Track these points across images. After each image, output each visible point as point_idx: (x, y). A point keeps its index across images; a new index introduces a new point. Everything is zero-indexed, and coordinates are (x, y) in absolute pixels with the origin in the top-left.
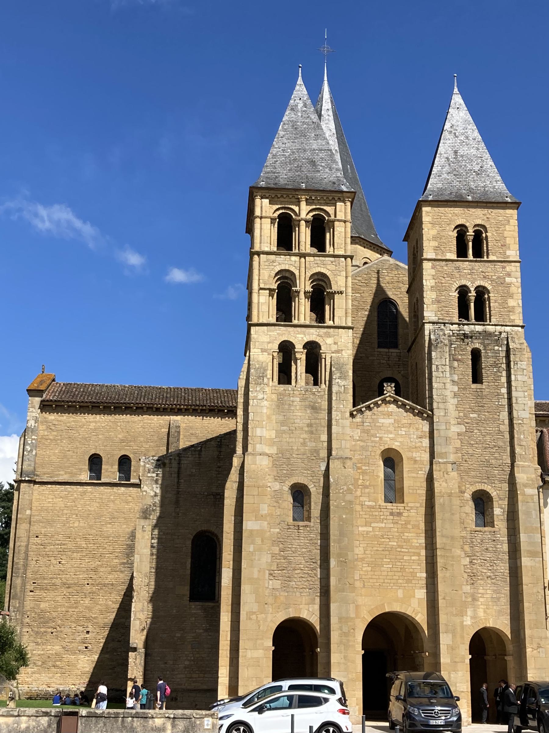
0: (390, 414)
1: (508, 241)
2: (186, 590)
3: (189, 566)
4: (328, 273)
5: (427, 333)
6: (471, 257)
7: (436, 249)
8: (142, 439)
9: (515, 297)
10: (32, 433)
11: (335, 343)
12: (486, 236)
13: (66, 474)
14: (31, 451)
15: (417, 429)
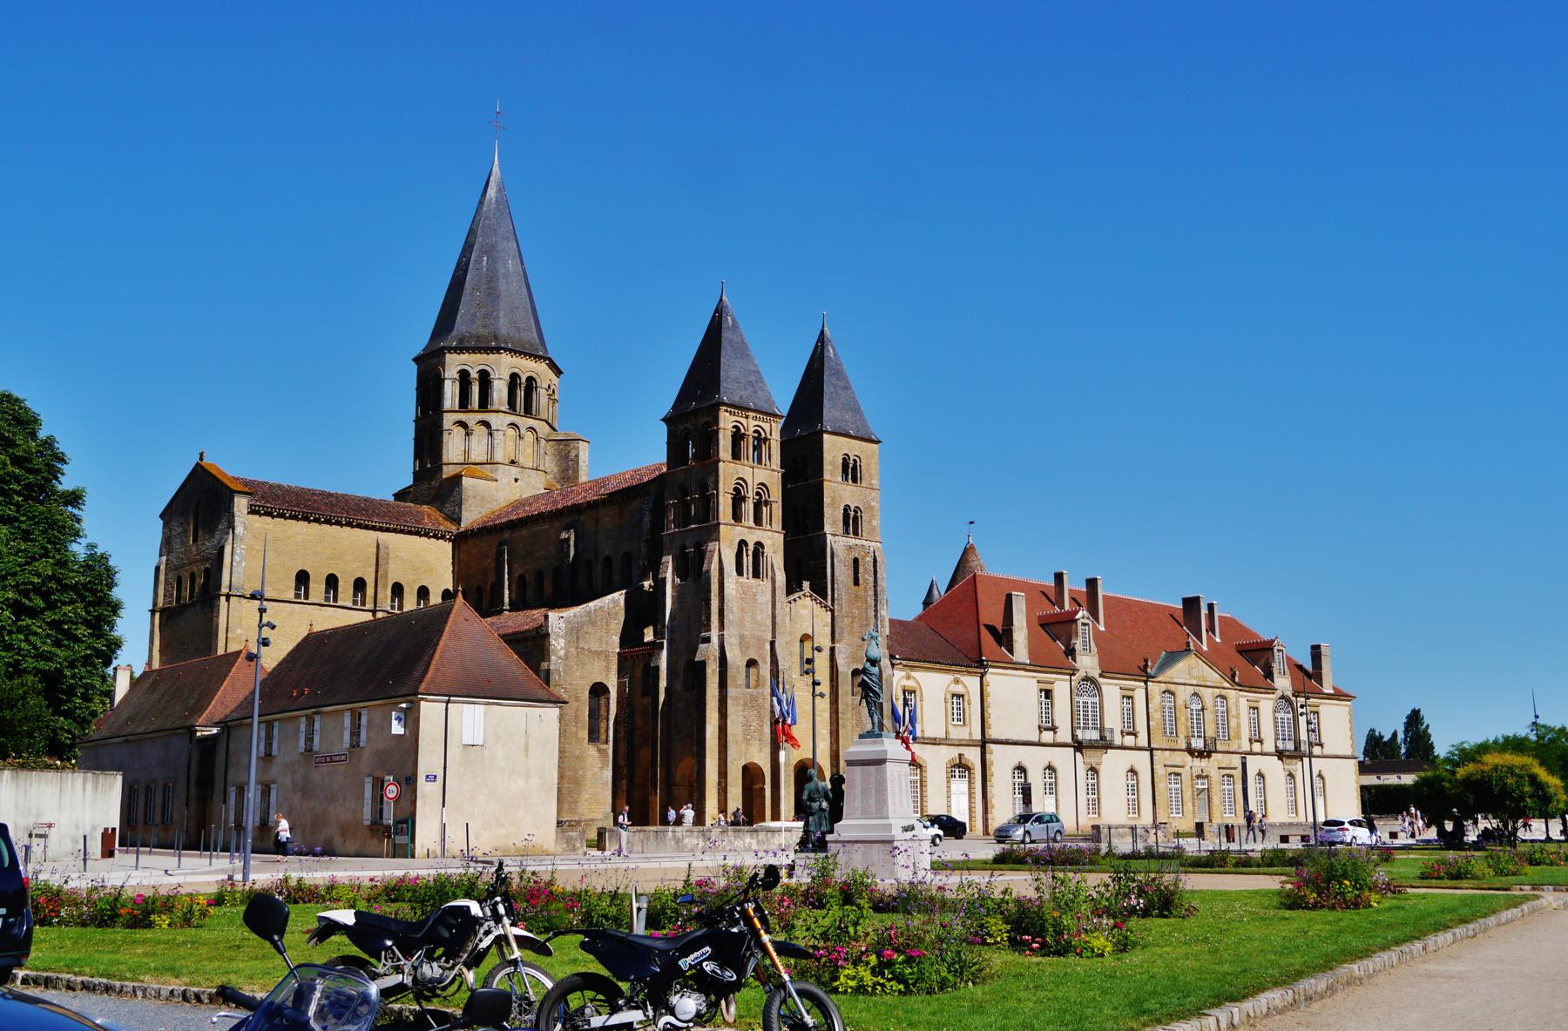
0: (805, 607)
1: (873, 472)
2: (585, 734)
3: (587, 713)
4: (768, 484)
5: (828, 542)
6: (850, 481)
7: (831, 474)
8: (349, 558)
9: (876, 517)
10: (241, 540)
11: (773, 545)
12: (860, 466)
13: (274, 589)
14: (240, 562)
15: (822, 619)
